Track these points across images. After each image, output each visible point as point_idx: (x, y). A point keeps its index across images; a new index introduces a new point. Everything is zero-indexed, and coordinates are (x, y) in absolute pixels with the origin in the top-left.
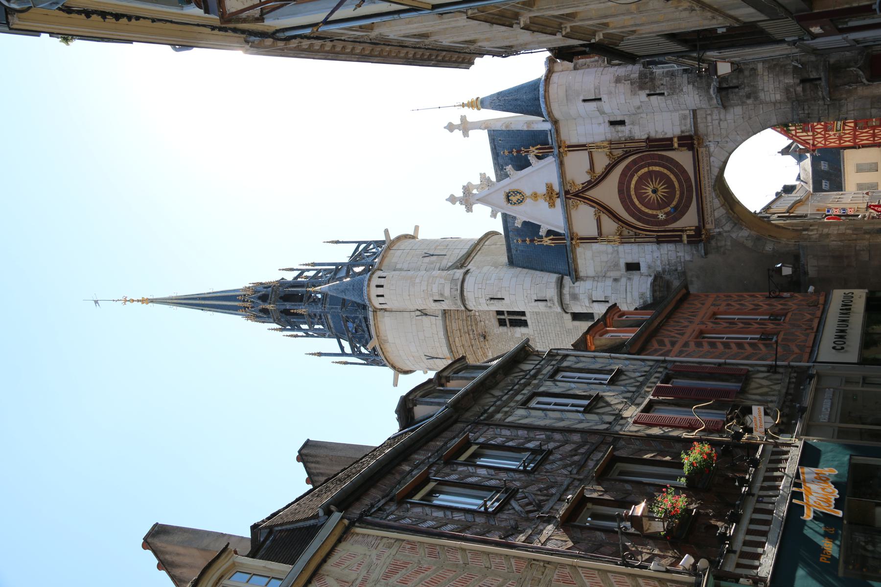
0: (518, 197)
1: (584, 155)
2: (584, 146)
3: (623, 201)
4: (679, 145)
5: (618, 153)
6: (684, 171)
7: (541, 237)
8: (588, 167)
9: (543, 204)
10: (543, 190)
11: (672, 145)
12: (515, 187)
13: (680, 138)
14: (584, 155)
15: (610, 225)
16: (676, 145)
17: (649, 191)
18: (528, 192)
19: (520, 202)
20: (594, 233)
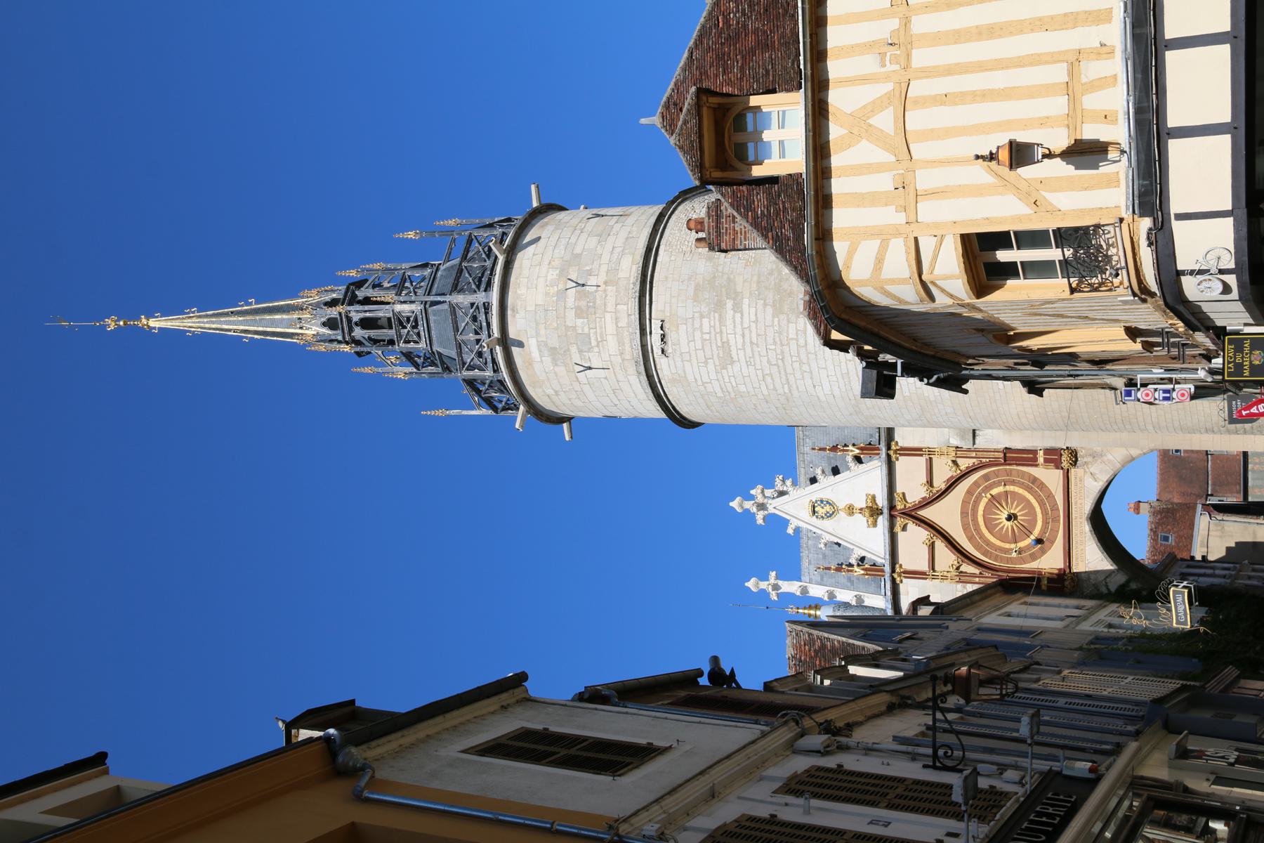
0: (828, 508)
1: (921, 461)
2: (920, 449)
3: (965, 527)
4: (1046, 461)
5: (964, 464)
6: (1050, 496)
7: (851, 565)
8: (923, 478)
9: (861, 520)
10: (861, 503)
11: (1036, 459)
12: (826, 495)
13: (1048, 451)
14: (921, 461)
15: (946, 558)
16: (1041, 460)
17: (1004, 515)
18: (841, 504)
19: (829, 515)
20: (924, 566)
